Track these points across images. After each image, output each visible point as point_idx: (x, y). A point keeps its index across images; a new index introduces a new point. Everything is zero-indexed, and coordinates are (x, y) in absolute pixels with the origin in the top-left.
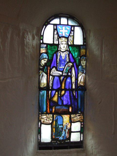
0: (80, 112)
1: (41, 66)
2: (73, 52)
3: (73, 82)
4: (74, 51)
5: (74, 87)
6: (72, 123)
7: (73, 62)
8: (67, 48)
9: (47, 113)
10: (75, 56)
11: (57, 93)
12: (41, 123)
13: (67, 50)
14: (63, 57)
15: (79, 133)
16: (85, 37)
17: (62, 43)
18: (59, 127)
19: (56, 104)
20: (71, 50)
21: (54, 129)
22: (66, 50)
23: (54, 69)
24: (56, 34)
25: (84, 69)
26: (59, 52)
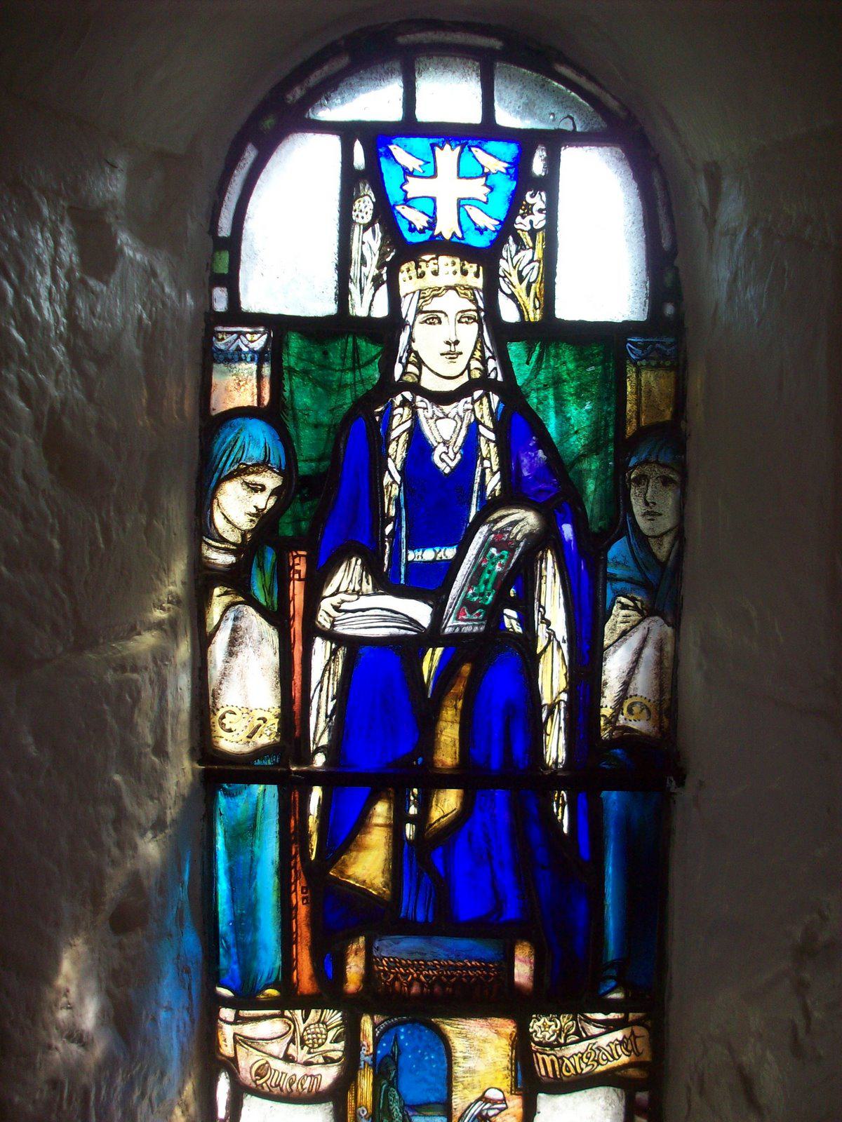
1: (224, 540)
2: (551, 402)
3: (546, 699)
4: (557, 382)
8: (484, 361)
9: (290, 999)
10: (565, 435)
11: (381, 810)
12: (239, 1091)
14: (440, 449)
16: (666, 244)
17: (434, 305)
20: (522, 373)
22: (476, 374)
24: (368, 218)
25: (662, 565)
26: (398, 400)
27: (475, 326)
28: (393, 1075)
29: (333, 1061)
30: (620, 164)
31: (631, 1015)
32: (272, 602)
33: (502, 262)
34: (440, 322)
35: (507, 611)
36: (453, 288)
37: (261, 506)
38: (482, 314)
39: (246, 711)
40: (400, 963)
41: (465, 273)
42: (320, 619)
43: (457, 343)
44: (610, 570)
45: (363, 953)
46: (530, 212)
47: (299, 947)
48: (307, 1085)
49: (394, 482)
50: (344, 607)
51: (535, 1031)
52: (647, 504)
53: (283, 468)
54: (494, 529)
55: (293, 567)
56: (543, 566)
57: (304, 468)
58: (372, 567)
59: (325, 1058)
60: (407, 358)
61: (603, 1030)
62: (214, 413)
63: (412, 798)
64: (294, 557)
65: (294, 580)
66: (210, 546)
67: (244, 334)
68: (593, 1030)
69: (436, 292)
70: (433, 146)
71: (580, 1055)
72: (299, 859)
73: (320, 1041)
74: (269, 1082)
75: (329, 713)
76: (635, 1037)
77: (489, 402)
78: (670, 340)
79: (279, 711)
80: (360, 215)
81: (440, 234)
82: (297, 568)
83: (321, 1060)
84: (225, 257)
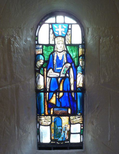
0: (79, 114)
3: (71, 83)
5: (72, 88)
6: (72, 125)
8: (64, 48)
9: (45, 115)
11: (54, 95)
12: (40, 125)
13: (64, 50)
15: (79, 135)
19: (54, 106)
20: (68, 50)
21: (53, 131)
22: (63, 50)
23: (51, 70)
26: (55, 52)
33: (66, 38)
41: (62, 39)
44: (78, 70)
45: (53, 110)
46: (69, 32)
57: (46, 60)
58: (53, 70)
68: (77, 118)
78: (84, 46)
84: (37, 38)
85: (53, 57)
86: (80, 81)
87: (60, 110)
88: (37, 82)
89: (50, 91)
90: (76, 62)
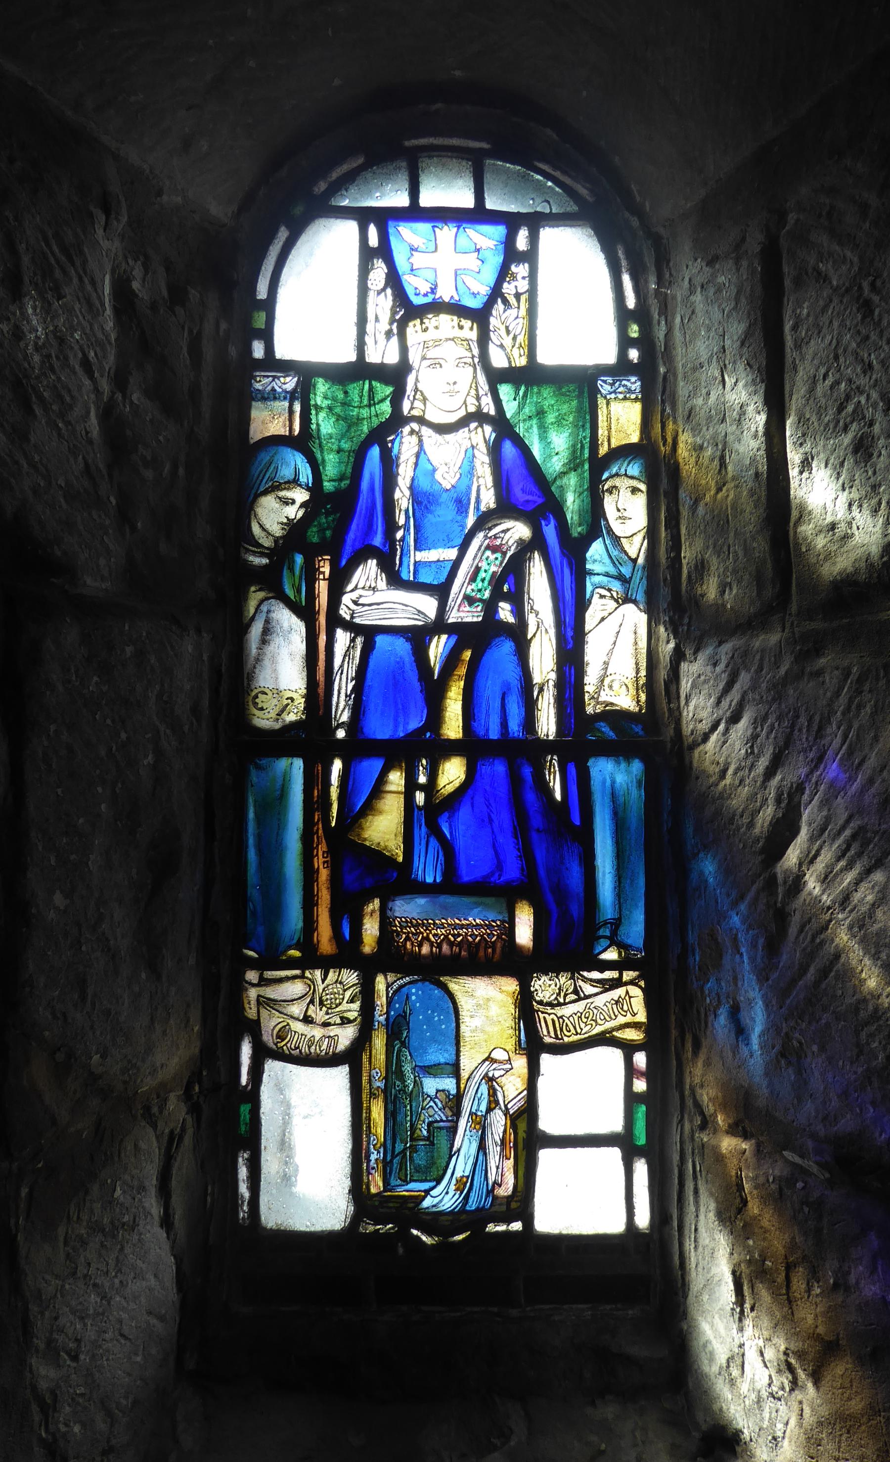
0: (611, 955)
1: (260, 546)
2: (535, 429)
3: (537, 679)
4: (540, 413)
5: (547, 724)
6: (546, 1060)
7: (531, 507)
8: (478, 398)
9: (312, 960)
11: (396, 779)
12: (262, 1054)
13: (479, 417)
15: (615, 1154)
18: (418, 1084)
20: (510, 408)
21: (377, 1112)
22: (472, 409)
23: (368, 572)
24: (381, 285)
25: (634, 561)
26: (406, 430)
27: (471, 369)
28: (405, 1035)
29: (349, 1021)
30: (590, 240)
31: (625, 973)
32: (300, 599)
33: (492, 320)
34: (441, 366)
35: (501, 604)
36: (453, 340)
37: (292, 516)
38: (476, 360)
39: (275, 692)
40: (411, 923)
41: (461, 327)
42: (341, 612)
43: (455, 383)
44: (588, 566)
45: (377, 915)
47: (320, 910)
48: (324, 1047)
49: (404, 496)
50: (361, 601)
51: (536, 990)
52: (619, 510)
53: (310, 485)
54: (489, 535)
55: (319, 567)
56: (532, 564)
59: (342, 1018)
60: (414, 397)
61: (600, 990)
62: (252, 442)
63: (421, 768)
64: (320, 561)
65: (319, 579)
66: (248, 550)
67: (278, 378)
68: (588, 989)
69: (437, 343)
70: (433, 227)
71: (579, 1014)
72: (320, 826)
73: (338, 1001)
74: (289, 1045)
75: (349, 693)
76: (630, 997)
77: (483, 431)
78: (633, 379)
79: (305, 691)
80: (374, 283)
81: (441, 297)
82: (321, 569)
83: (338, 1021)
84: (263, 315)
85: (389, 464)
86: (606, 664)
87: (448, 911)
88: (251, 661)
89: (358, 747)
90: (572, 502)
